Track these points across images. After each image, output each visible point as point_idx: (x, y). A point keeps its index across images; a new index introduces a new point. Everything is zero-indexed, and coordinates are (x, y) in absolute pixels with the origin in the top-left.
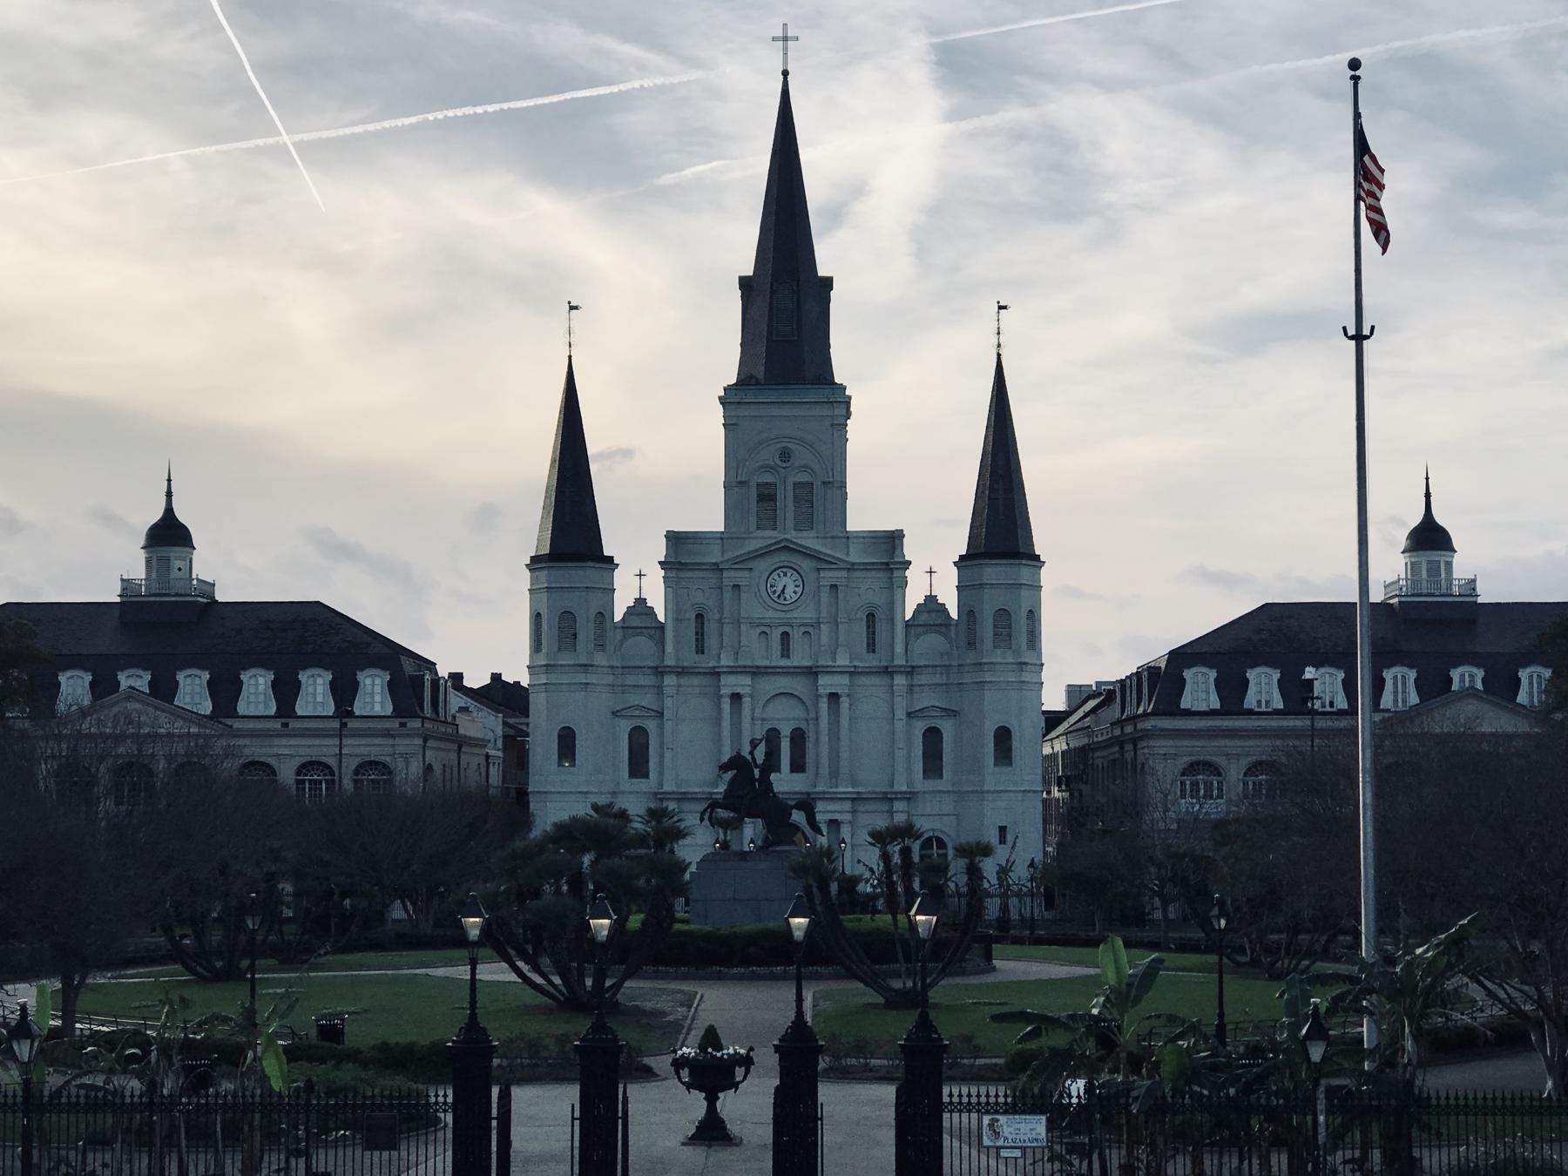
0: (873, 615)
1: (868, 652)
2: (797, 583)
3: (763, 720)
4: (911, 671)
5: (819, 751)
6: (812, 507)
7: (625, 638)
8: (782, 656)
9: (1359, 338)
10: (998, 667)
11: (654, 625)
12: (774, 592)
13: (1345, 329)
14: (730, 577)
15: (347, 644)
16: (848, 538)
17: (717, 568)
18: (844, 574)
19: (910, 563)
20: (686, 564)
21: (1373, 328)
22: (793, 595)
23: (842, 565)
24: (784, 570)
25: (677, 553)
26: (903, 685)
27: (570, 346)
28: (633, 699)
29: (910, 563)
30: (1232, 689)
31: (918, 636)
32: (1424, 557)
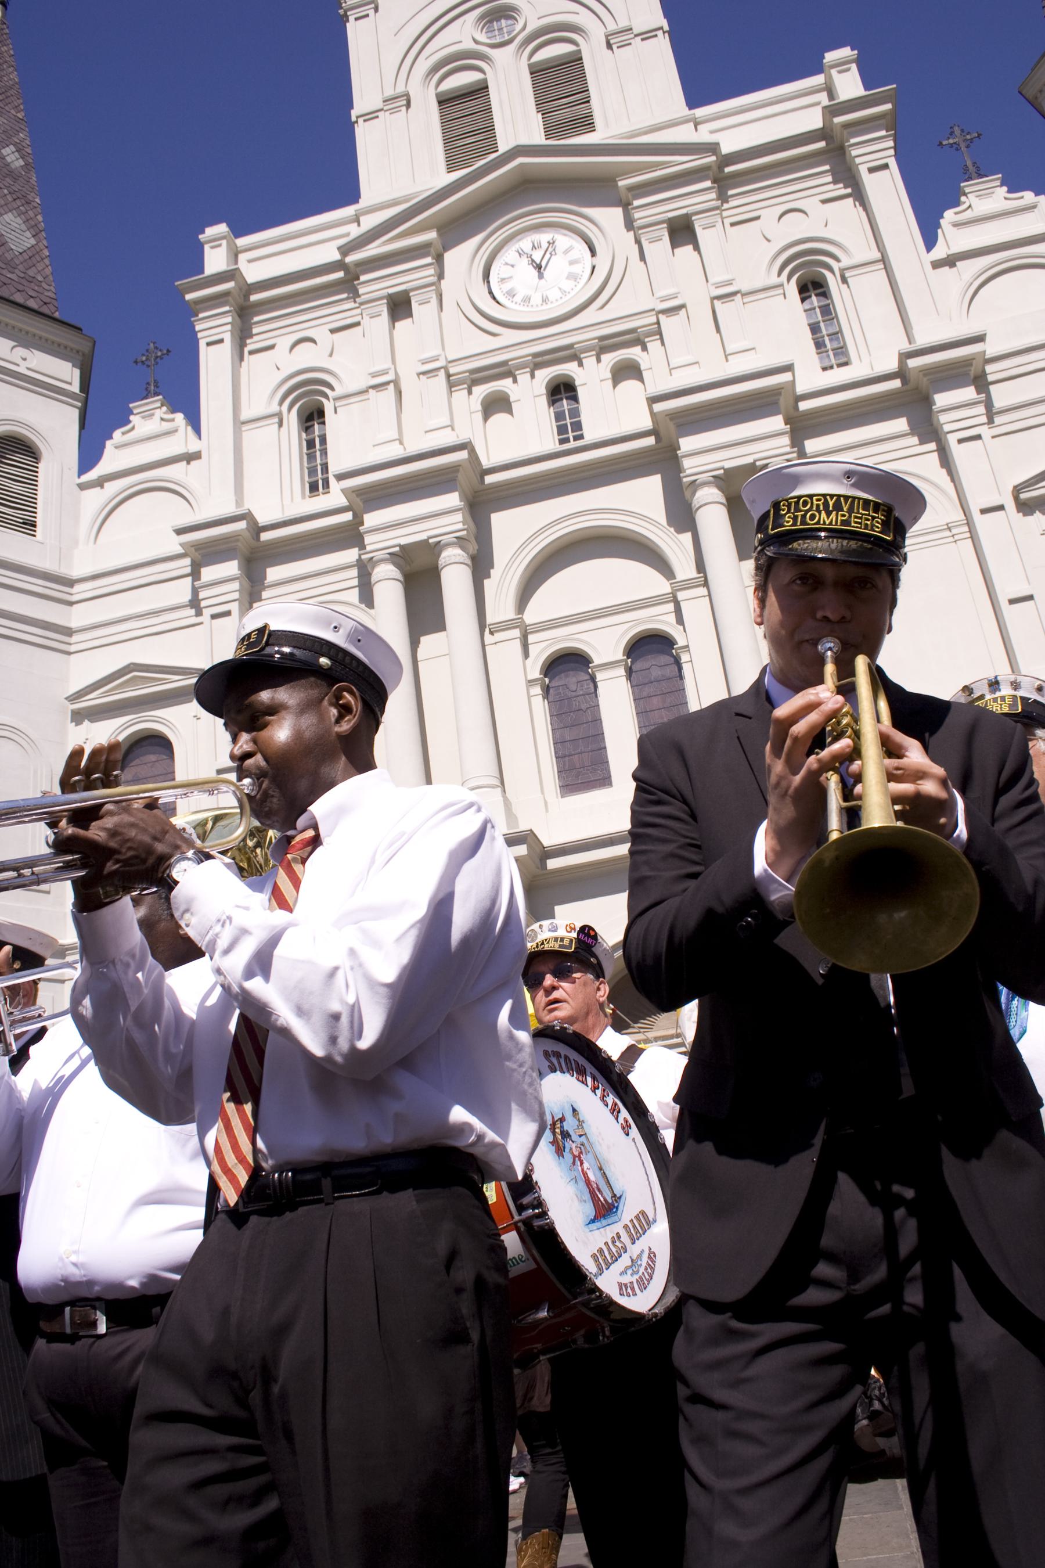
8: (562, 442)
12: (511, 294)
22: (567, 285)
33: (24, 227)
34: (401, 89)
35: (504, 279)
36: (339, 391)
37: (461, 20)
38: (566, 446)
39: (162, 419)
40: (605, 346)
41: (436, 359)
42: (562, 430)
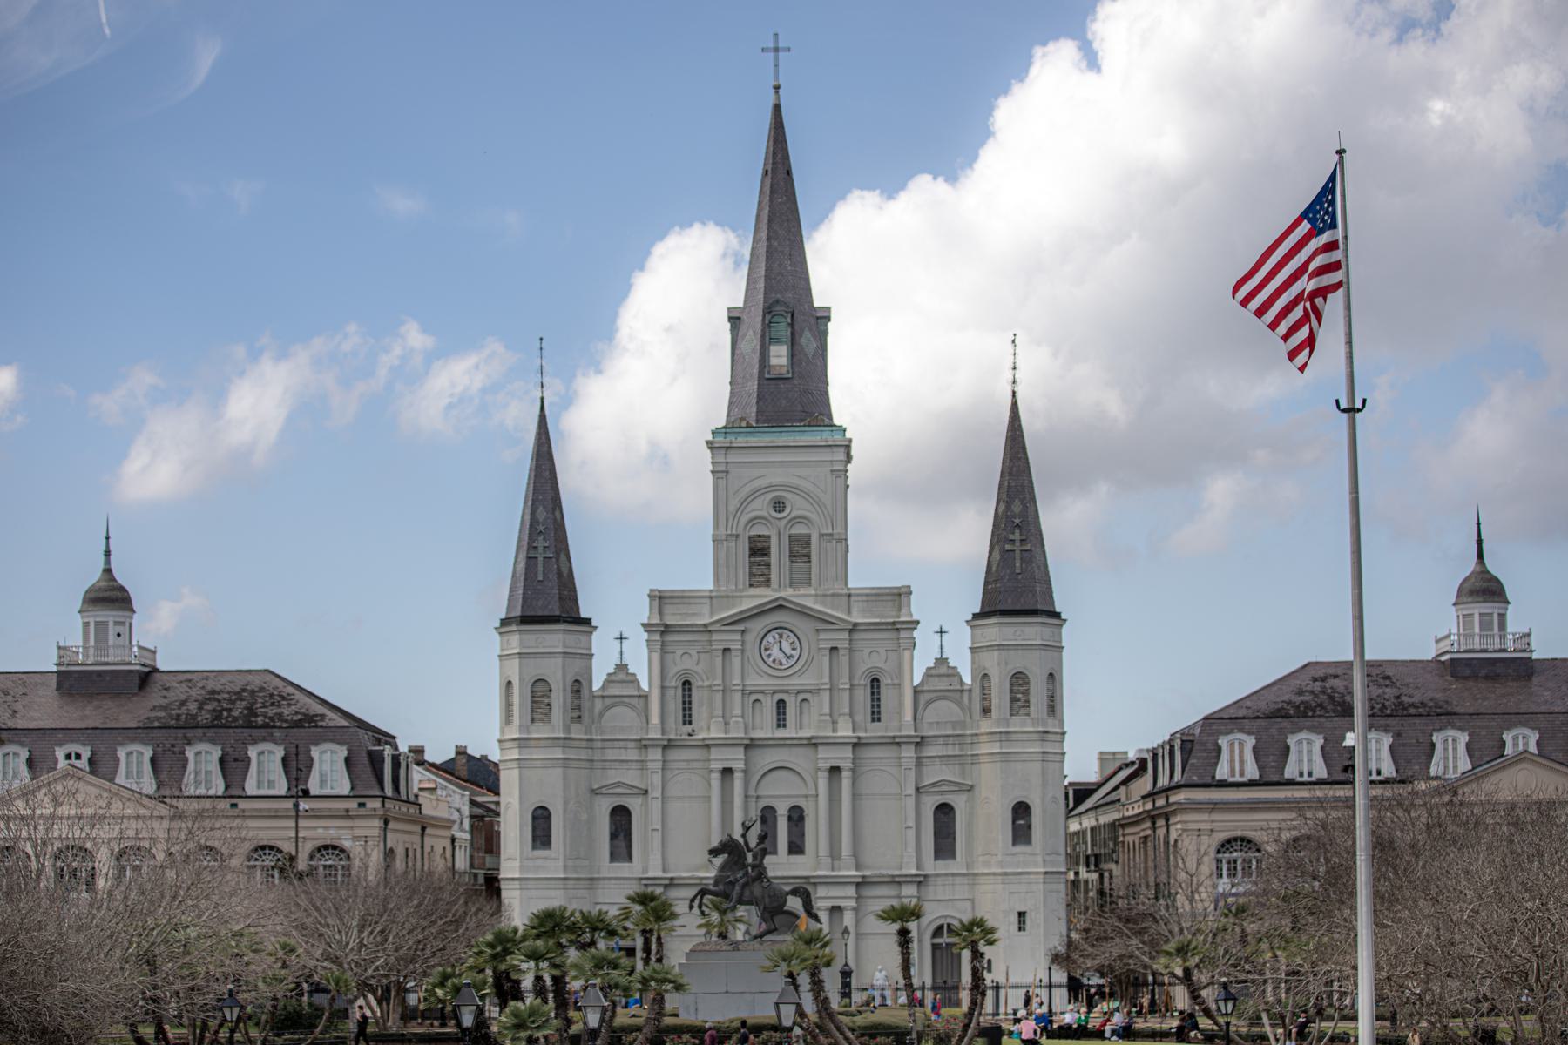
0: (878, 680)
1: (873, 720)
3: (758, 797)
4: (920, 743)
5: (816, 832)
6: (810, 562)
8: (779, 726)
9: (1351, 410)
10: (1014, 737)
11: (636, 693)
12: (769, 656)
13: (1337, 401)
15: (299, 717)
16: (849, 595)
17: (706, 629)
18: (845, 635)
19: (918, 622)
21: (1364, 401)
23: (842, 625)
24: (778, 631)
25: (661, 613)
26: (911, 757)
27: (542, 386)
28: (614, 776)
29: (918, 622)
30: (1272, 754)
31: (929, 703)
32: (1477, 609)
34: (734, 532)
36: (700, 683)
37: (763, 497)
41: (738, 685)
42: (779, 720)
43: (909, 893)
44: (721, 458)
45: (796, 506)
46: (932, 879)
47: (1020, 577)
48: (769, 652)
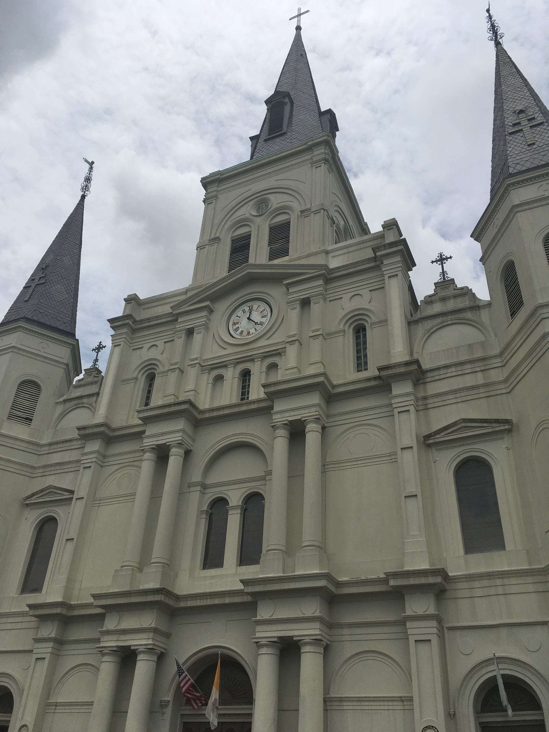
2: (265, 313)
7: (63, 415)
8: (242, 399)
12: (236, 330)
14: (185, 323)
20: (141, 321)
23: (313, 273)
24: (249, 304)
26: (407, 395)
31: (430, 333)
33: (64, 290)
35: (235, 323)
37: (247, 205)
38: (244, 402)
39: (94, 376)
40: (265, 356)
43: (420, 611)
44: (213, 188)
45: (275, 201)
46: (460, 585)
47: (535, 146)
48: (237, 326)
